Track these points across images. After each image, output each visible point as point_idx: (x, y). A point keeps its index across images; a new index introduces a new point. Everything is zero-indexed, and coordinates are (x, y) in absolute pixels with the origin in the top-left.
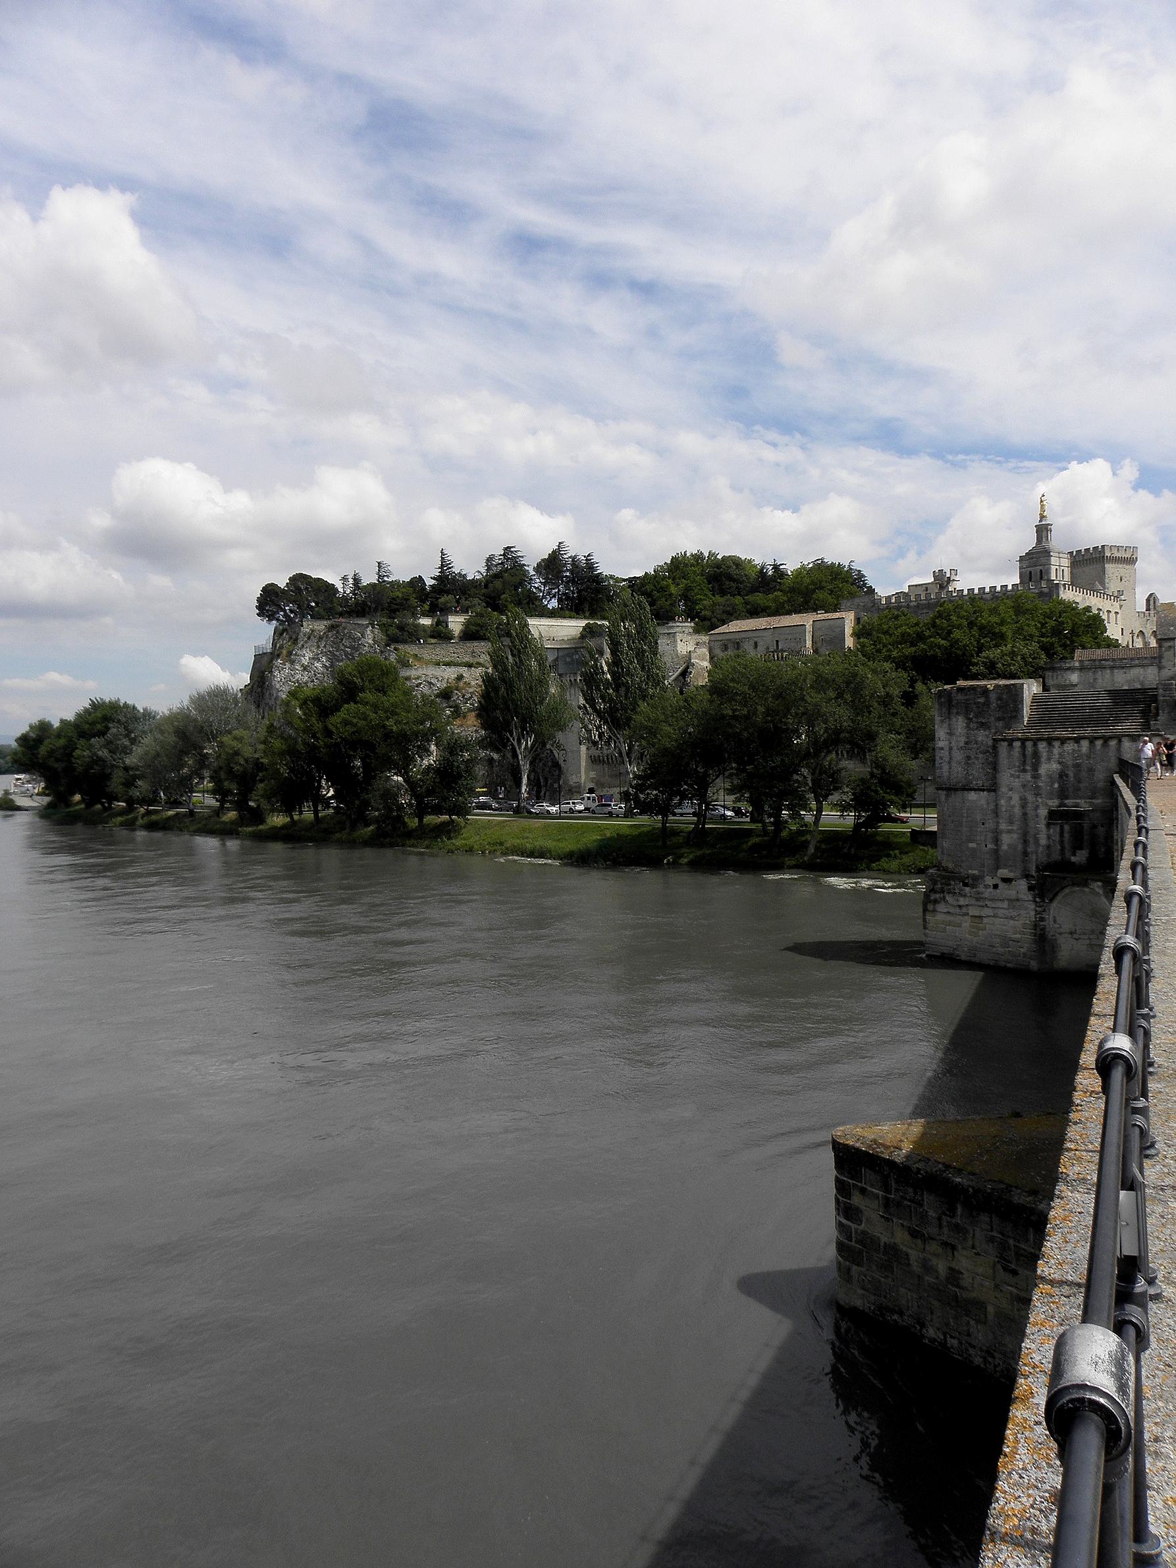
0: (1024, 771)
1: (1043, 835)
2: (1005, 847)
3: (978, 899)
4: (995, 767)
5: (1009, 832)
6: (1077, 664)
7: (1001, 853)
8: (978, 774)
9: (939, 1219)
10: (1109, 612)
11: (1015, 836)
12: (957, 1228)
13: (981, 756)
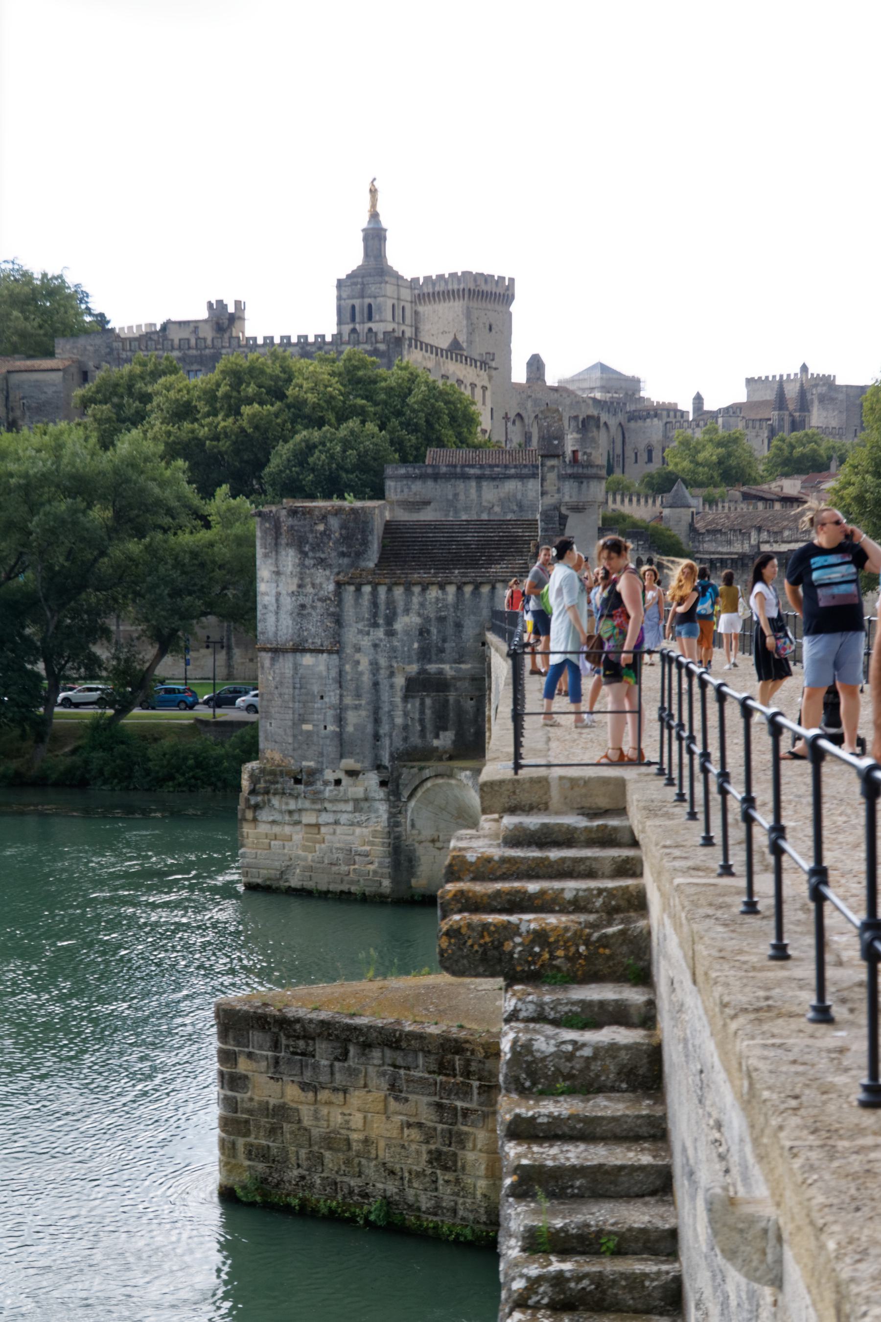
0: (375, 625)
1: (399, 712)
2: (350, 729)
3: (314, 802)
4: (338, 621)
5: (357, 707)
6: (430, 471)
7: (345, 736)
8: (316, 629)
9: (332, 1066)
10: (473, 386)
11: (364, 713)
12: (352, 1072)
13: (319, 604)
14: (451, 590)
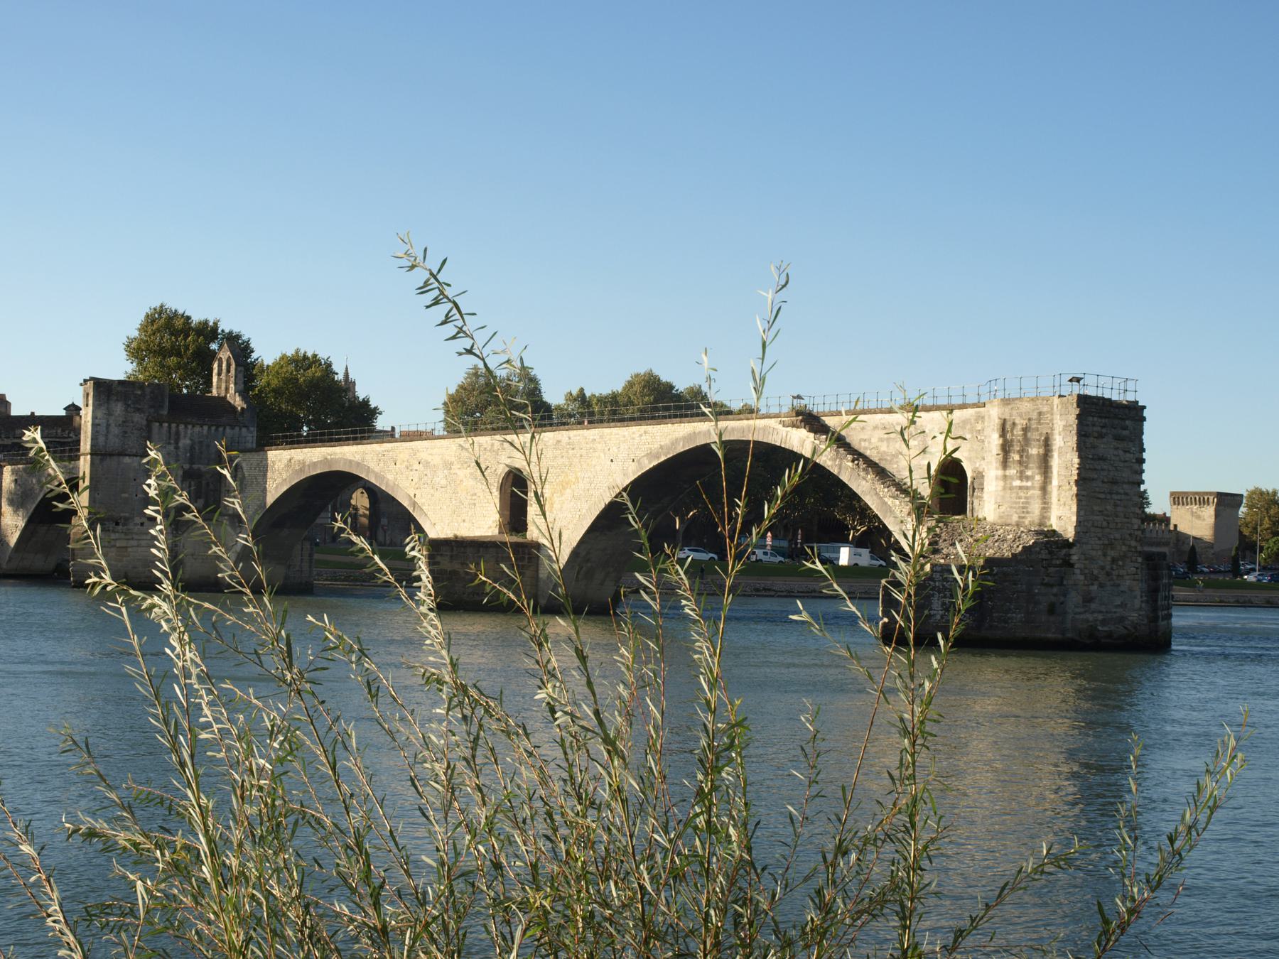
3: (126, 534)
14: (206, 428)
